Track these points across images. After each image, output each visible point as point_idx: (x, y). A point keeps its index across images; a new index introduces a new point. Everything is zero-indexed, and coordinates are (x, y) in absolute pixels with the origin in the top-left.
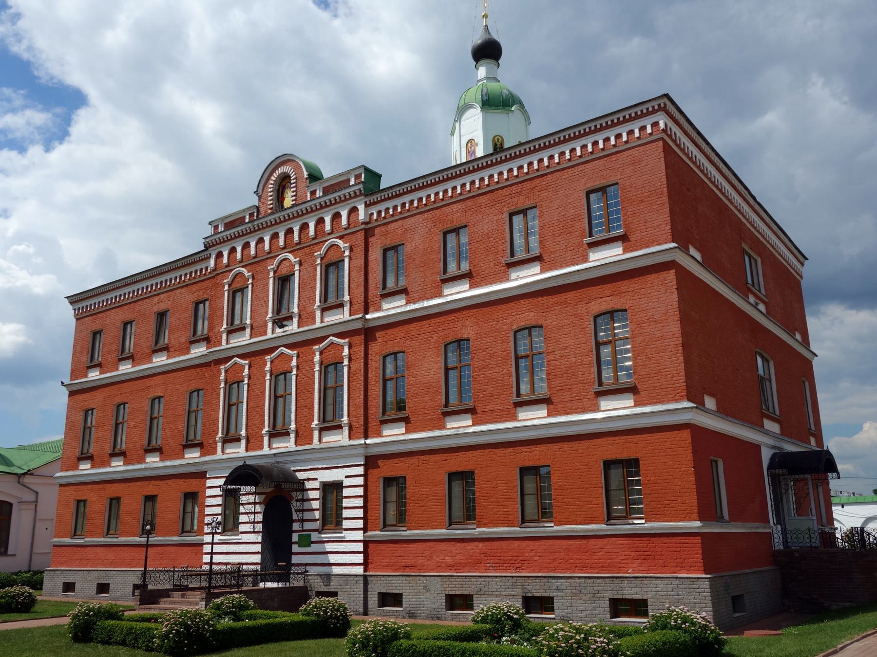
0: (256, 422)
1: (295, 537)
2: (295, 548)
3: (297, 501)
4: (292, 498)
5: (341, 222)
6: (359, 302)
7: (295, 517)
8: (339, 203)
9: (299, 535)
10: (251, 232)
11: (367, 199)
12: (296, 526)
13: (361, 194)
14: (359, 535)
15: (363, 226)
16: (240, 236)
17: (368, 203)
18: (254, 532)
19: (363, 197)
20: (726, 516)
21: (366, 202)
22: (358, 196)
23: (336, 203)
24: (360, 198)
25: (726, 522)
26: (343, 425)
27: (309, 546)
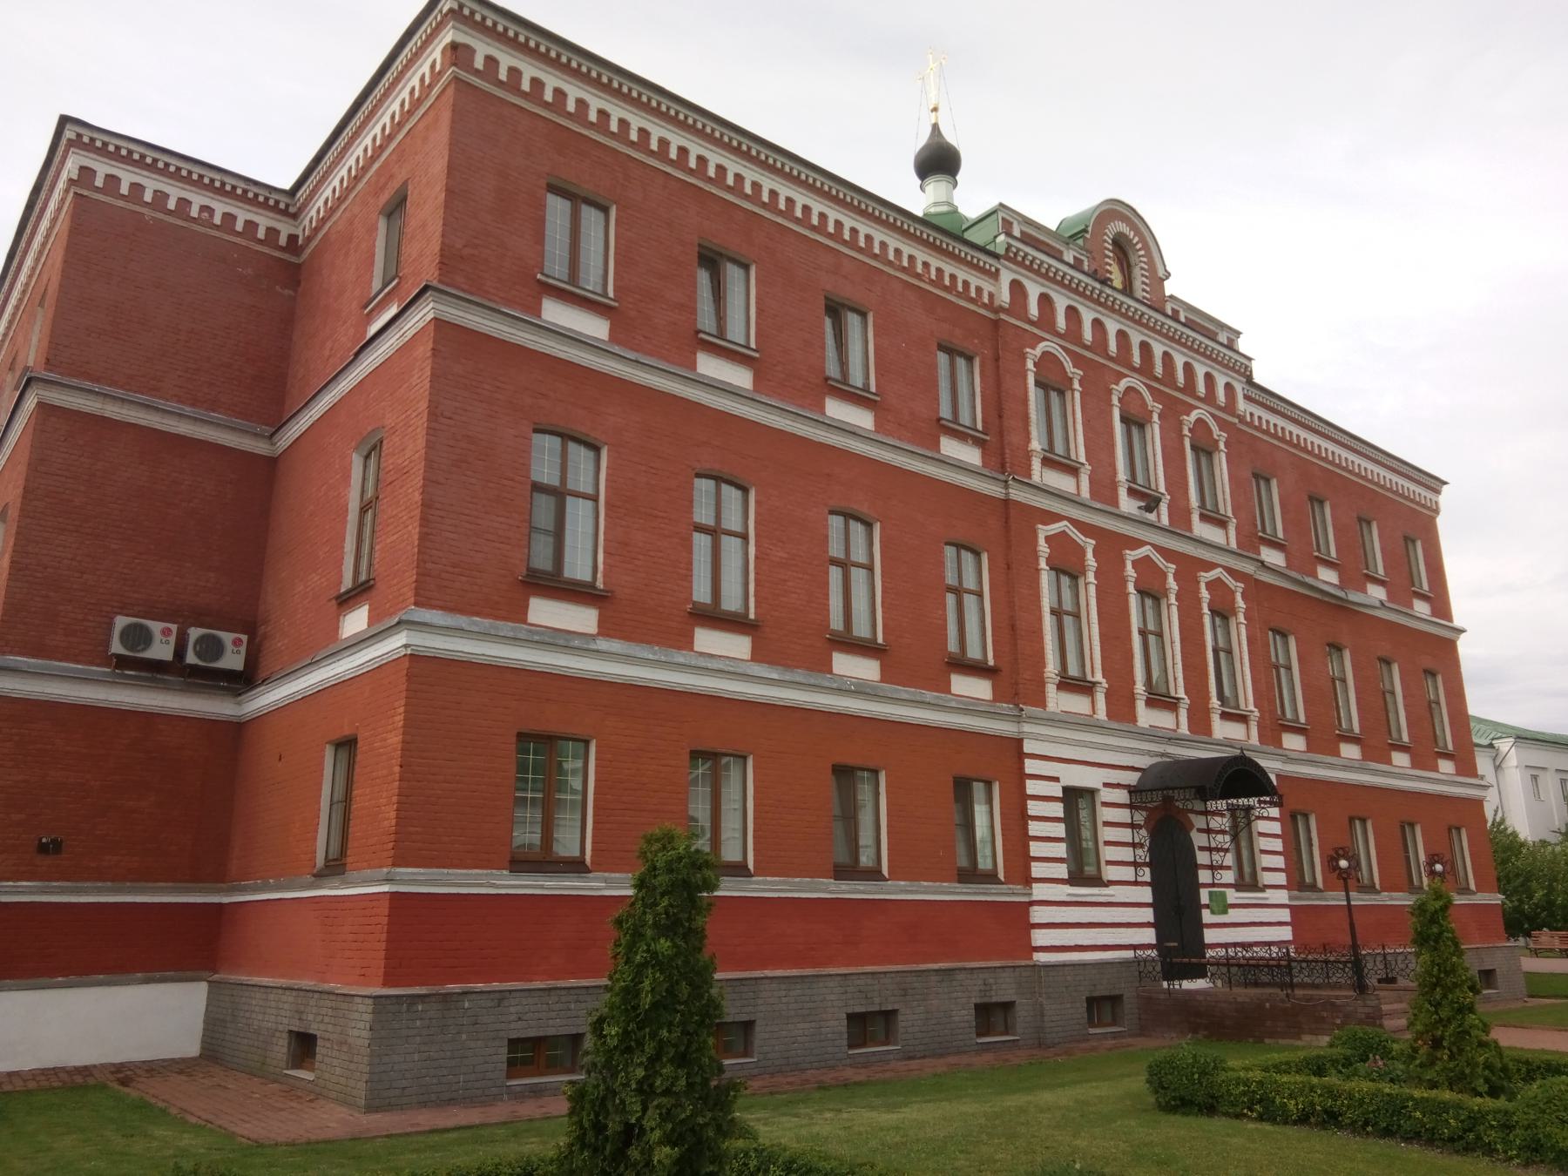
1: (1204, 896)
2: (1207, 916)
3: (1200, 830)
4: (1192, 826)
7: (1202, 858)
9: (1210, 892)
12: (1204, 876)
14: (1282, 897)
18: (1136, 883)
20: (1473, 886)
25: (1321, 891)
27: (1225, 912)
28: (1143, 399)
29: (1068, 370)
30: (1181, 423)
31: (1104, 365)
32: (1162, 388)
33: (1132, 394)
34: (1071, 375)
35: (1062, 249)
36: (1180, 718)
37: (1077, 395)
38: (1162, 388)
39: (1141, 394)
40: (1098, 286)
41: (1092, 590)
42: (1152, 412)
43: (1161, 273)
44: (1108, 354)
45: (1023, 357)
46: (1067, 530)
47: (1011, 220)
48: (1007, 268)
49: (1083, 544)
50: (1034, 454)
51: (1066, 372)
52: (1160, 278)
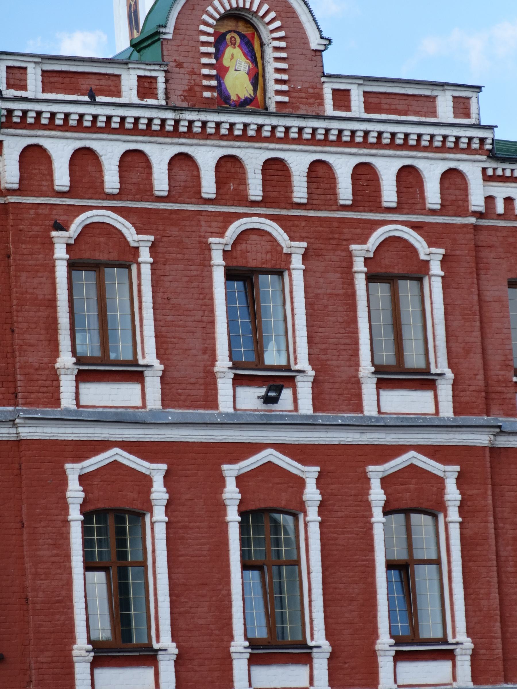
0: (201, 622)
5: (423, 197)
6: (472, 388)
8: (425, 149)
10: (162, 132)
11: (490, 165)
13: (480, 150)
15: (472, 220)
16: (122, 130)
17: (490, 172)
19: (484, 158)
21: (484, 170)
22: (475, 152)
23: (418, 147)
24: (478, 157)
26: (458, 651)
28: (273, 240)
29: (129, 239)
30: (349, 258)
31: (199, 213)
32: (312, 213)
33: (254, 238)
34: (133, 244)
35: (116, 72)
36: (316, 672)
37: (146, 271)
38: (312, 213)
39: (269, 234)
40: (169, 115)
41: (161, 531)
42: (289, 255)
43: (315, 43)
44: (201, 198)
45: (50, 245)
46: (120, 459)
47: (23, 65)
48: (8, 135)
49: (148, 473)
50: (62, 371)
51: (128, 243)
52: (316, 51)
